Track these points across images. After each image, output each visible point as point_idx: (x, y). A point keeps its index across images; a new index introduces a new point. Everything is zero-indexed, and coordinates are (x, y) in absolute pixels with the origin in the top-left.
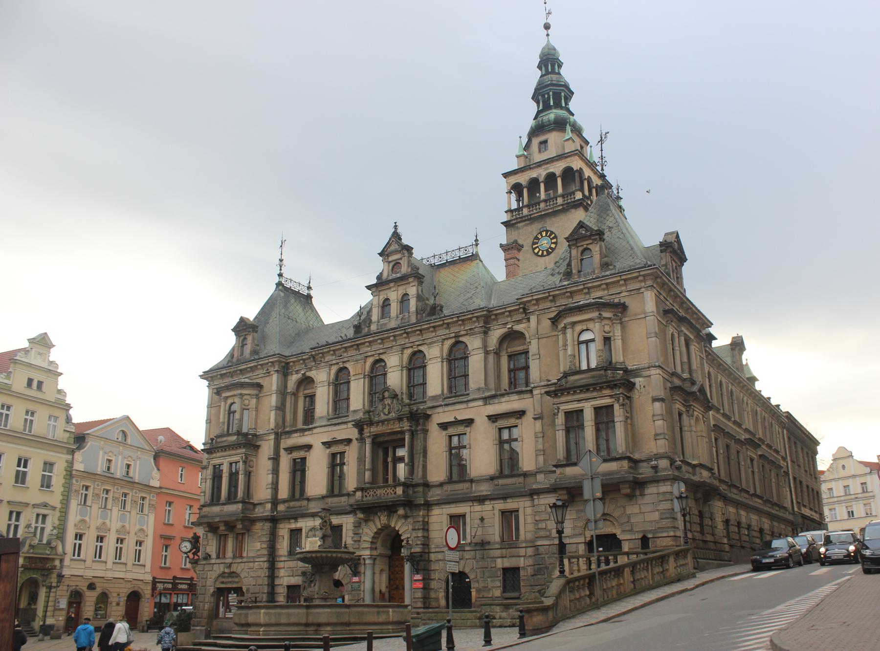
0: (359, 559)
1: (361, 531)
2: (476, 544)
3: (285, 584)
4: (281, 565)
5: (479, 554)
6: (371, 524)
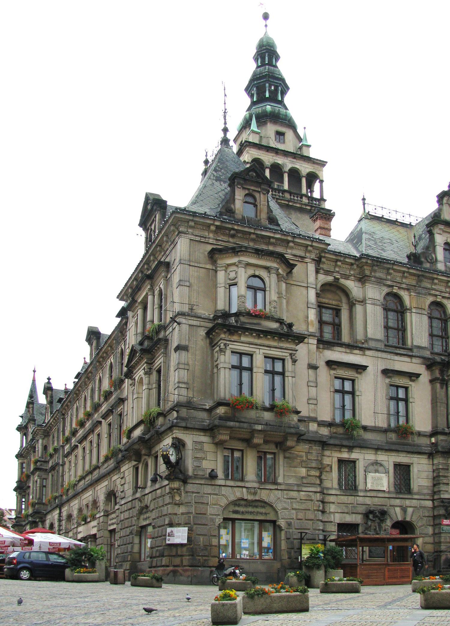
3: (338, 521)
4: (332, 499)
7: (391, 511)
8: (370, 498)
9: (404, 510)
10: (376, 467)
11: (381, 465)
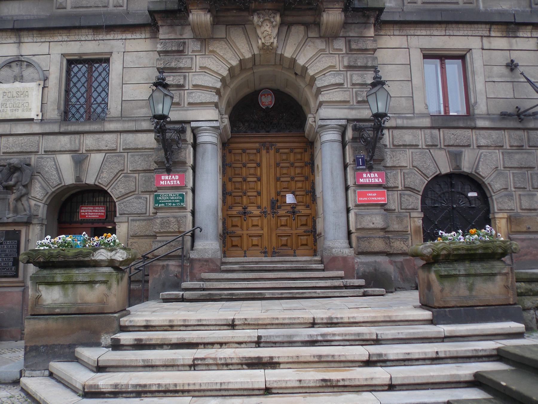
0: (183, 131)
1: (184, 63)
2: (504, 116)
5: (507, 139)
6: (219, 48)
7: (48, 164)
9: (80, 160)
10: (16, 69)
11: (29, 64)
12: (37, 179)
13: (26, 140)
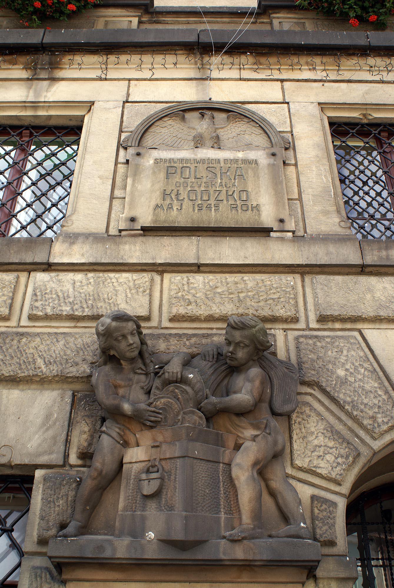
8: (144, 278)
12: (308, 404)
13: (250, 284)
